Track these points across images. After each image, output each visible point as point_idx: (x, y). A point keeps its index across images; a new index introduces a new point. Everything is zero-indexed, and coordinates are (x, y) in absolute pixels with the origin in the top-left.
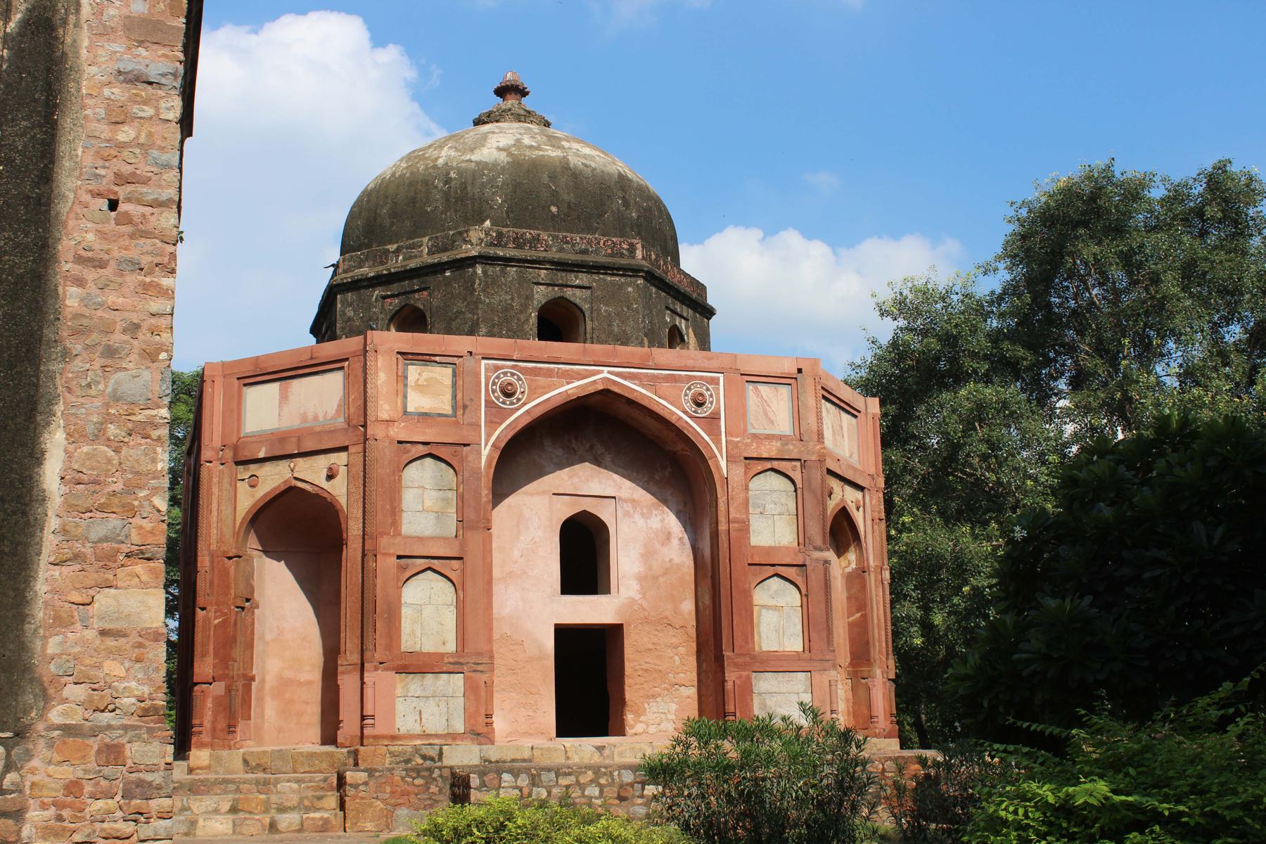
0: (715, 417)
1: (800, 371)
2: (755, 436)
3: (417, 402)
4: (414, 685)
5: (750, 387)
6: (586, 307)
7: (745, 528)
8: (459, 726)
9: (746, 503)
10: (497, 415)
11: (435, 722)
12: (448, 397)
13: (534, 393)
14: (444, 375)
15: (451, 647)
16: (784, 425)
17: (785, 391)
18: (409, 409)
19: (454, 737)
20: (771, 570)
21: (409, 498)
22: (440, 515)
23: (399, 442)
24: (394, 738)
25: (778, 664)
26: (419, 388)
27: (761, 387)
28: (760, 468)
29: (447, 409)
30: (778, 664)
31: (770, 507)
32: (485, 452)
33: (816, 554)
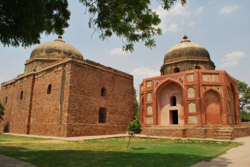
0: (182, 81)
1: (194, 71)
2: (188, 82)
3: (148, 86)
4: (148, 118)
5: (187, 76)
6: (179, 68)
7: (187, 96)
8: (153, 123)
9: (187, 92)
10: (156, 86)
11: (150, 123)
12: (151, 85)
13: (160, 82)
14: (150, 82)
15: (152, 114)
16: (192, 80)
17: (192, 75)
18: (148, 87)
19: (152, 124)
20: (190, 102)
21: (148, 97)
22: (151, 99)
23: (146, 91)
24: (146, 124)
25: (192, 114)
26: (148, 84)
27: (189, 75)
28: (189, 87)
29: (151, 86)
30: (192, 114)
31: (191, 92)
32: (155, 90)
33: (197, 98)
